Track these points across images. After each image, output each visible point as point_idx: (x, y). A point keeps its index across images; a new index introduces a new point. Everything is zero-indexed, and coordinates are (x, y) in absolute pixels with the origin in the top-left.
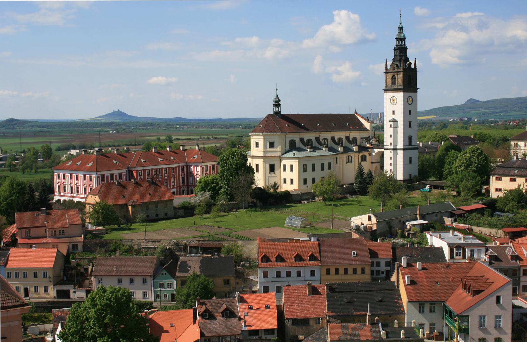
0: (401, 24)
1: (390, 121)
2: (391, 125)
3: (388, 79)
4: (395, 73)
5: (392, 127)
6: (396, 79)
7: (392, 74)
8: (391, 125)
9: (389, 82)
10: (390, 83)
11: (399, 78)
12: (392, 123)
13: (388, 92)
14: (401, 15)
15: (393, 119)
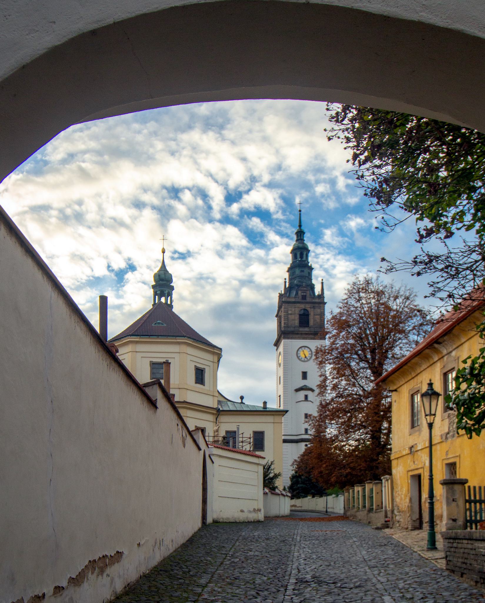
0: (300, 226)
1: (297, 390)
2: (306, 397)
3: (291, 314)
4: (308, 307)
5: (309, 399)
6: (308, 315)
7: (303, 306)
8: (306, 397)
9: (294, 320)
10: (297, 322)
11: (317, 315)
12: (309, 393)
13: (292, 338)
14: (300, 211)
15: (305, 386)
